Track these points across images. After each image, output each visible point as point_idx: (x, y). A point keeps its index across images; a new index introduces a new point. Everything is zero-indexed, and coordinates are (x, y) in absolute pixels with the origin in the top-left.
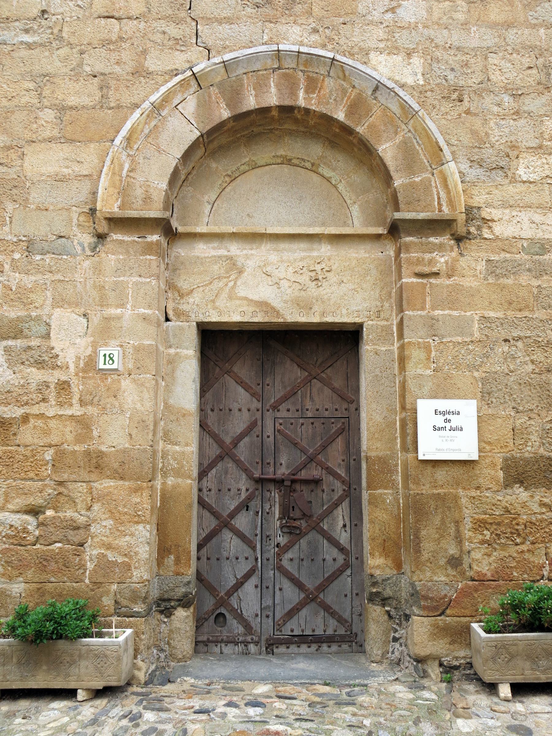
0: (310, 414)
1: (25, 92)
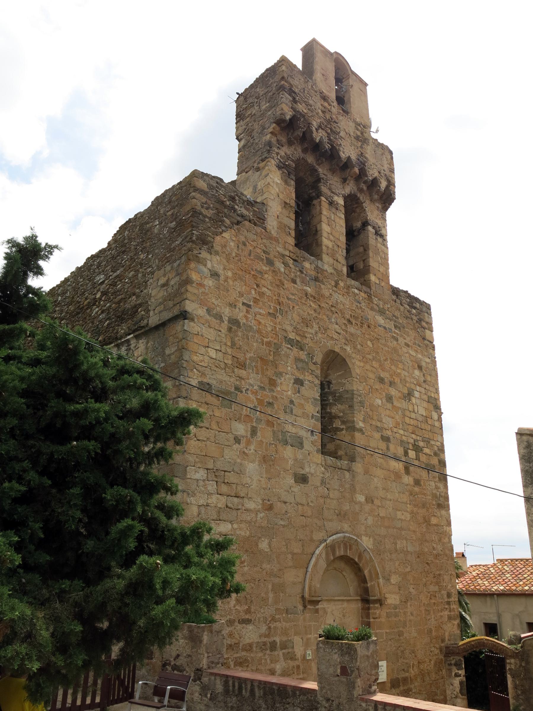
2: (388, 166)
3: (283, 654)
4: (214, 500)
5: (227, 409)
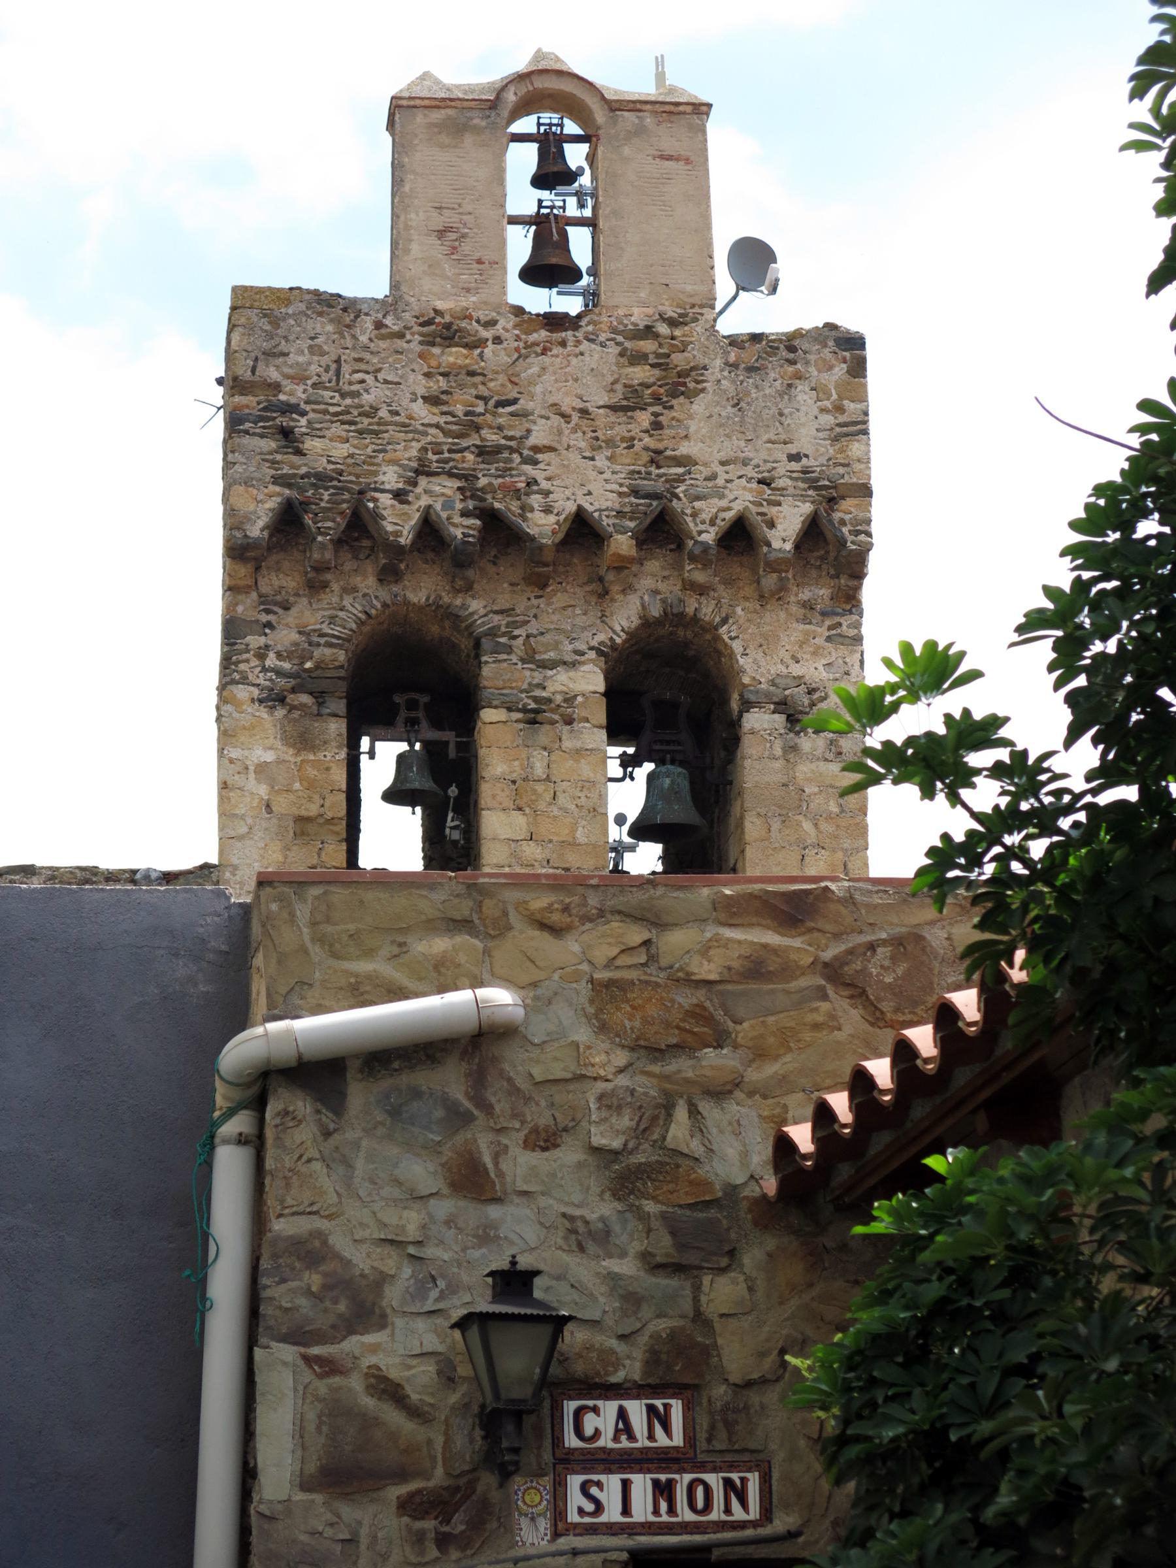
2: (828, 420)
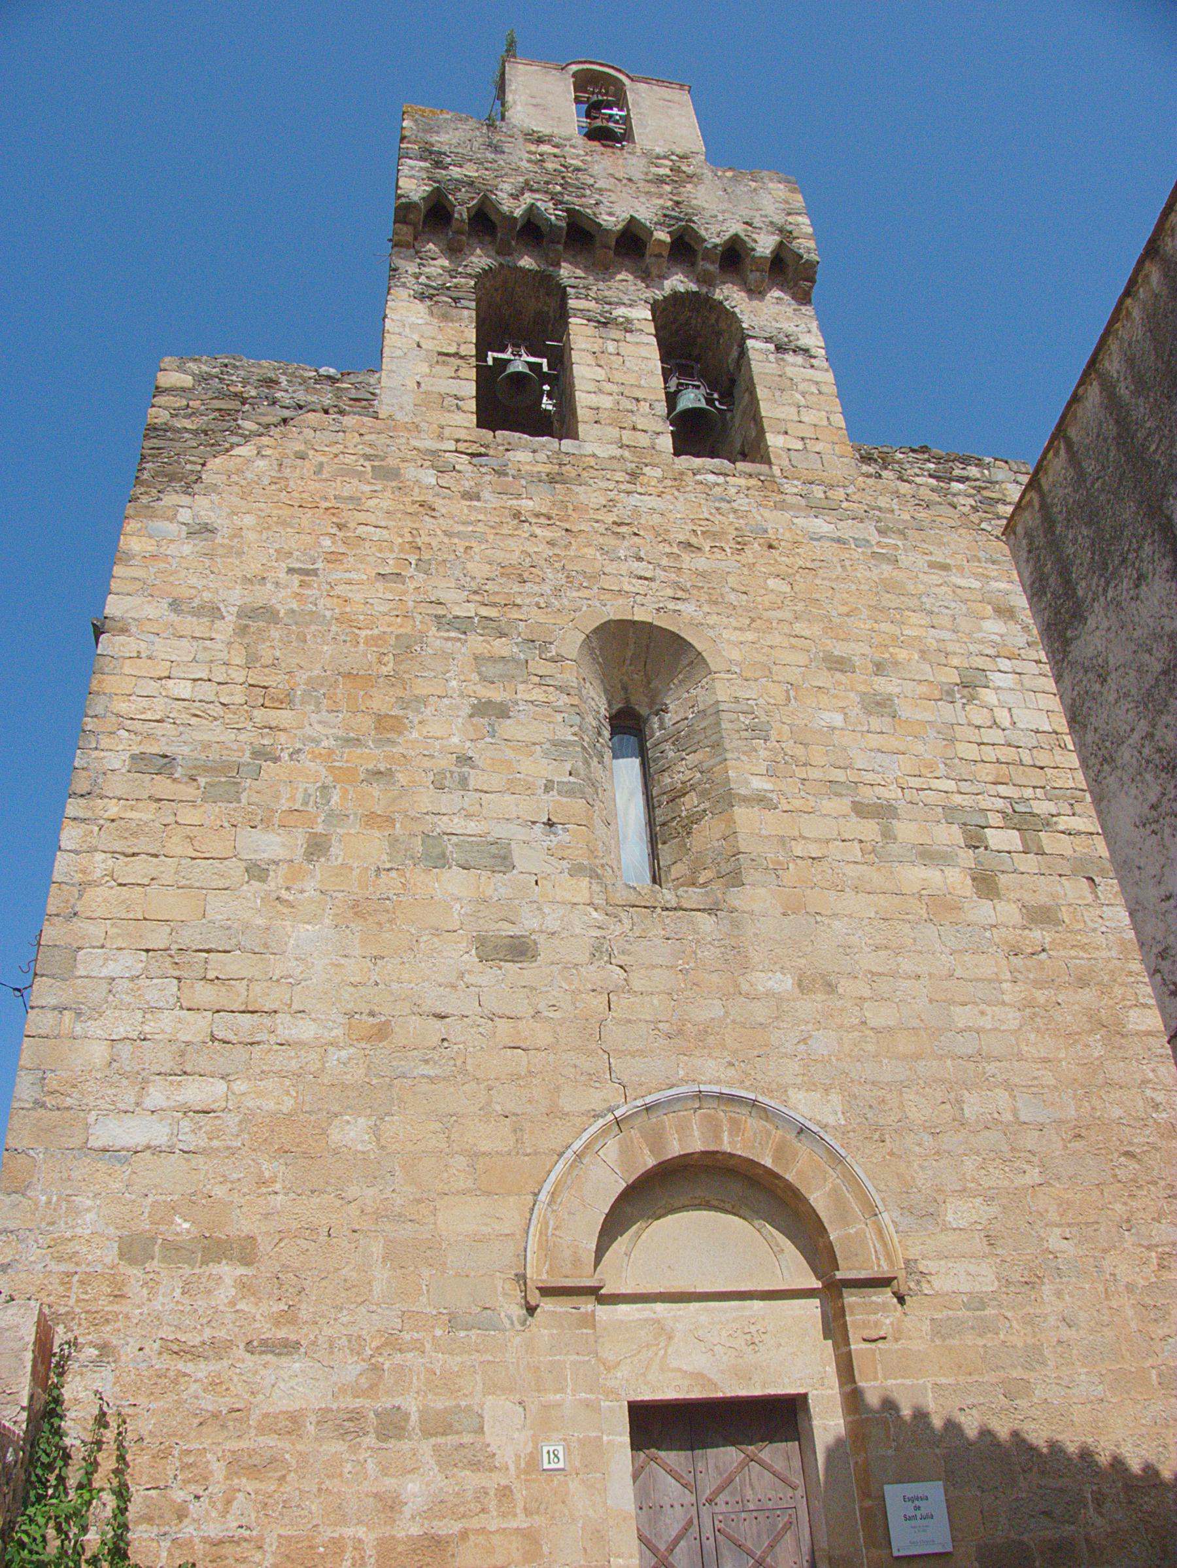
0: (752, 1507)
1: (431, 1135)
3: (436, 1448)
4: (165, 1023)
5: (220, 804)
